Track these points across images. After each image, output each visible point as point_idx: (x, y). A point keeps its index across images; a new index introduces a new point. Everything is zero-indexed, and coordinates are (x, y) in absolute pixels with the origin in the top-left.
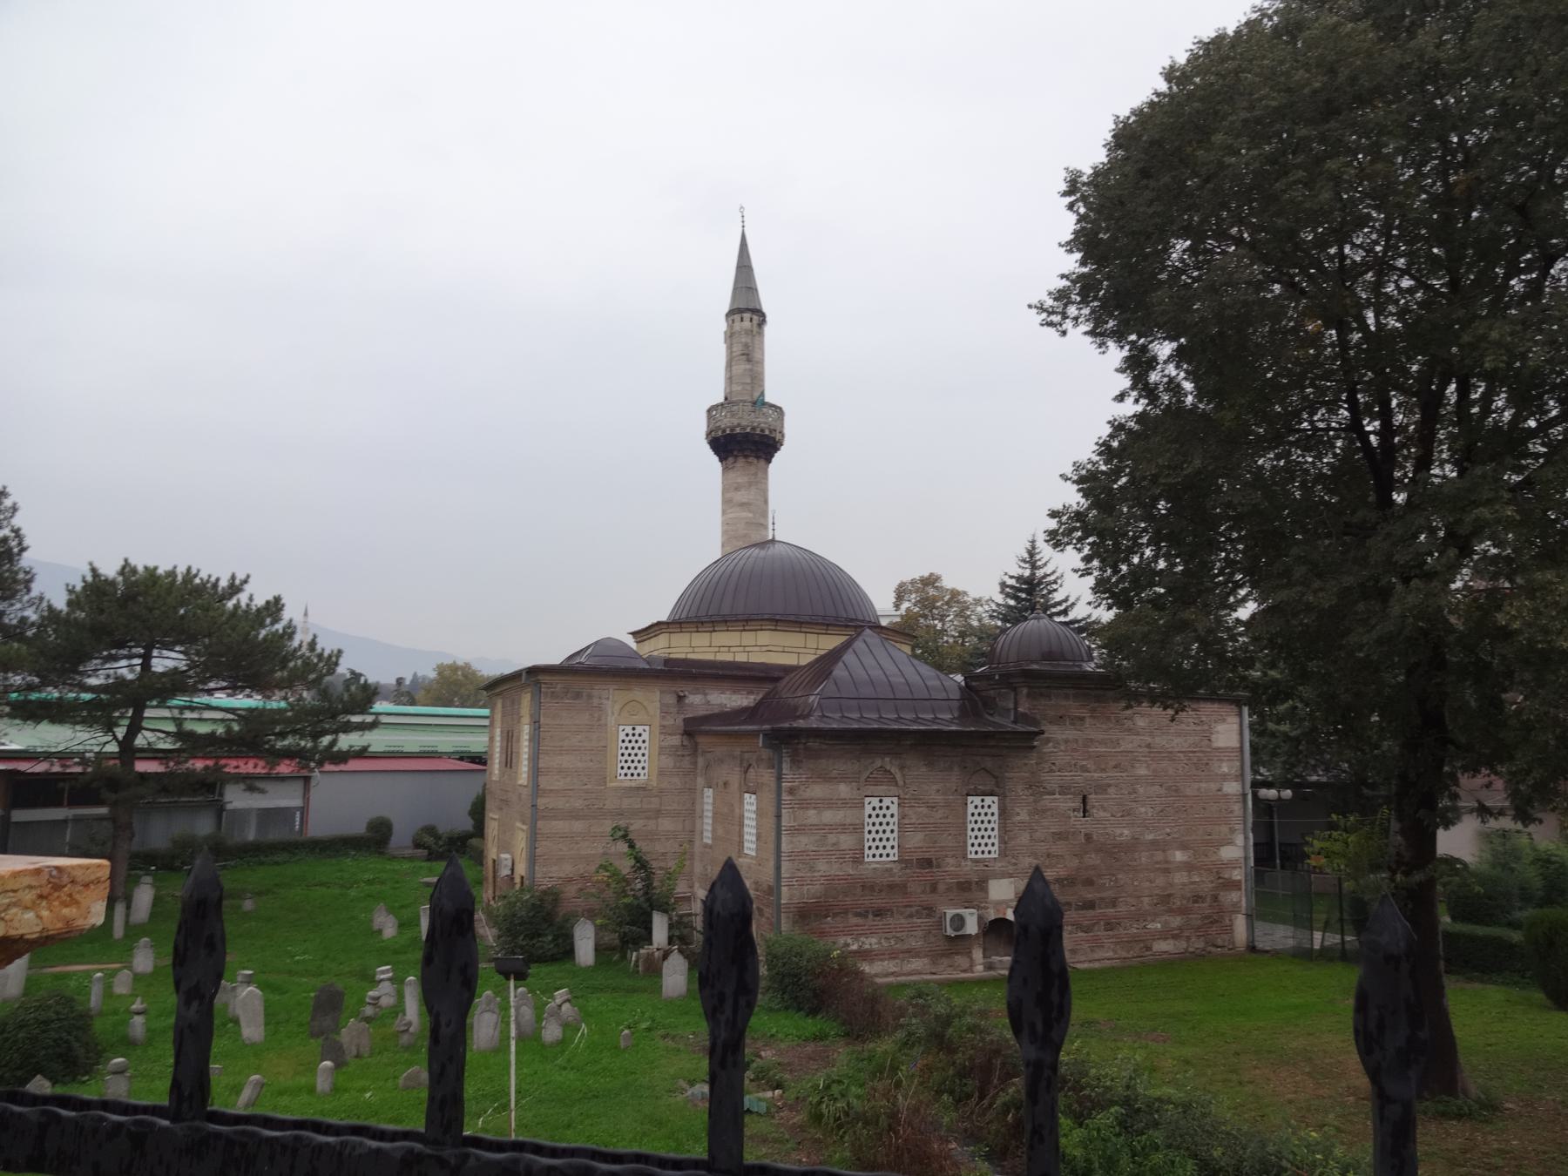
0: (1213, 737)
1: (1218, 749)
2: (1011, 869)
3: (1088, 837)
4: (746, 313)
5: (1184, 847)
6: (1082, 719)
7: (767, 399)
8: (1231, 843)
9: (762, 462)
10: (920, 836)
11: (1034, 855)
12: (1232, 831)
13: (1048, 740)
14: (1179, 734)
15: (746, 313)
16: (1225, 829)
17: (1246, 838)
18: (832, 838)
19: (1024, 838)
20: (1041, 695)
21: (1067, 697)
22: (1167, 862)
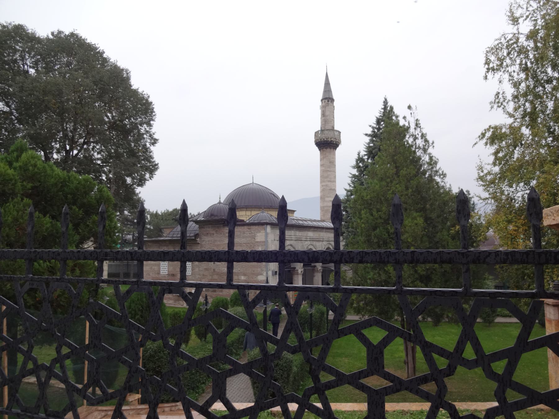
0: (256, 238)
1: (257, 242)
2: (194, 278)
3: (214, 270)
4: (328, 99)
5: (245, 275)
6: (213, 234)
7: (335, 129)
8: (262, 274)
9: (332, 150)
10: (172, 268)
11: (199, 274)
12: (262, 270)
13: (204, 241)
14: (243, 237)
15: (328, 99)
16: (259, 269)
17: (267, 273)
18: (153, 267)
19: (197, 270)
20: (202, 227)
21: (209, 227)
22: (239, 279)
